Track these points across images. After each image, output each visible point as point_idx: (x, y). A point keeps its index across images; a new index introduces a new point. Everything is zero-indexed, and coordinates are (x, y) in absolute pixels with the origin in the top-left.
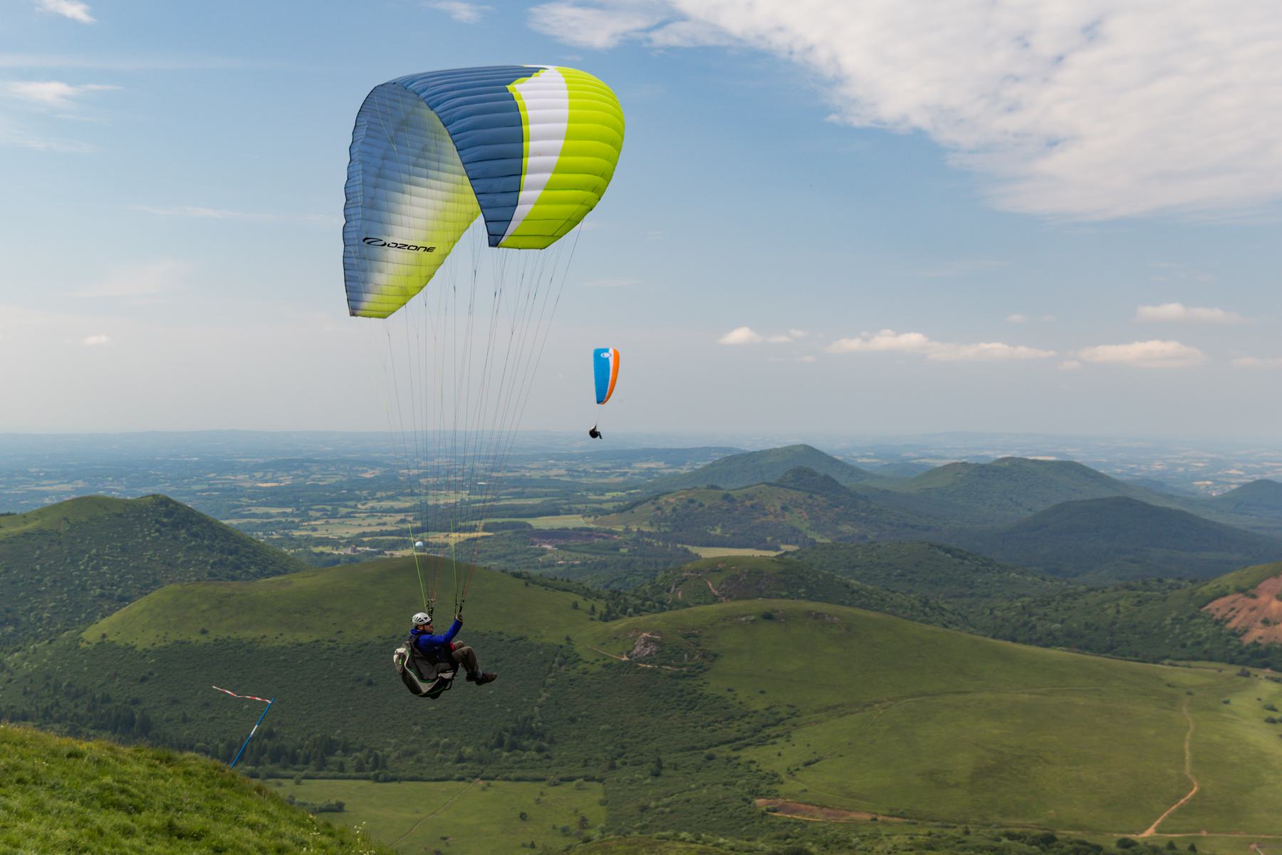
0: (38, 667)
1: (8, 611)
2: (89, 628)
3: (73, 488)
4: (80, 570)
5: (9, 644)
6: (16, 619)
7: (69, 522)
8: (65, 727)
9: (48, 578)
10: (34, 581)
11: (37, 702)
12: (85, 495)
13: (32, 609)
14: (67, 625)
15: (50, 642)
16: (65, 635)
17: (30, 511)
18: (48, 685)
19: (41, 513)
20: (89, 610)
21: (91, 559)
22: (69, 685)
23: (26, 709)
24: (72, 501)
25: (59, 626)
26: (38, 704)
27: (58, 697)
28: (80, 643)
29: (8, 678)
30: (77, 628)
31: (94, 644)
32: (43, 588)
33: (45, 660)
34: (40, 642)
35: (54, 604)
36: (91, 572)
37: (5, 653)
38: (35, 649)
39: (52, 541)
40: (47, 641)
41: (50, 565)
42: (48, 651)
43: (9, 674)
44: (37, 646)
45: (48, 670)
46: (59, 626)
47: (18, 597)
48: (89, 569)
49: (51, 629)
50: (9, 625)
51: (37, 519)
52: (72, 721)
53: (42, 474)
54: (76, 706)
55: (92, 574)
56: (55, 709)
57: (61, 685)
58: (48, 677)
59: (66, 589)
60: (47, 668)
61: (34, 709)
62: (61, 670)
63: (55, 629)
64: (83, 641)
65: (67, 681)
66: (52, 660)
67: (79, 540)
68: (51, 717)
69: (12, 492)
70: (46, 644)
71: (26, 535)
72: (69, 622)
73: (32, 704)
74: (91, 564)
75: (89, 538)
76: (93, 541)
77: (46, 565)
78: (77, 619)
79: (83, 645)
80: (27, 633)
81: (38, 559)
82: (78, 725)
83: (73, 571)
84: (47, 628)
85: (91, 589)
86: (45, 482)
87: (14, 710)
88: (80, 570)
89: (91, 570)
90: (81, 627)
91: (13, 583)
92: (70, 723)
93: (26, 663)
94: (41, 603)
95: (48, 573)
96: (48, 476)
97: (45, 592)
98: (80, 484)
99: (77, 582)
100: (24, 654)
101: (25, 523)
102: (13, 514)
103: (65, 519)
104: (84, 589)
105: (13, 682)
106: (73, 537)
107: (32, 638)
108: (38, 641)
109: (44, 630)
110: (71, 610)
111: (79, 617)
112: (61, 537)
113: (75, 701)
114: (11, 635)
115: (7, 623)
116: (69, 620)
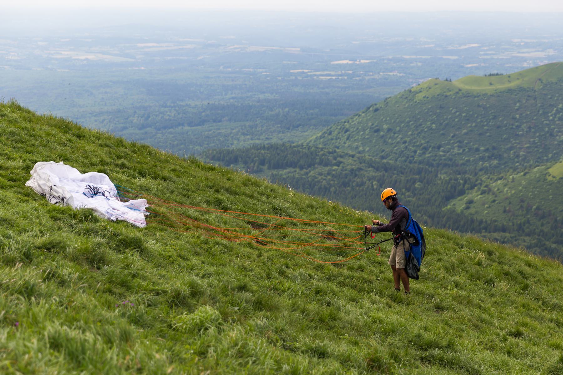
0: (515, 193)
1: (494, 148)
2: (555, 165)
3: (545, 55)
4: (549, 120)
5: (494, 174)
6: (500, 155)
7: (542, 82)
8: (534, 240)
9: (525, 125)
10: (514, 127)
11: (513, 219)
12: (554, 62)
13: (511, 148)
14: (538, 162)
15: (525, 175)
16: (536, 170)
17: (513, 72)
18: (522, 207)
19: (521, 75)
20: (555, 152)
21: (558, 112)
22: (538, 208)
23: (505, 223)
24: (546, 65)
25: (532, 162)
26: (515, 221)
27: (529, 216)
28: (547, 176)
29: (492, 199)
30: (545, 165)
31: (558, 178)
32: (521, 133)
33: (520, 188)
34: (517, 174)
35: (528, 145)
36: (557, 122)
37: (491, 180)
38: (513, 178)
39: (529, 96)
40: (522, 174)
41: (527, 115)
42: (523, 181)
43: (494, 196)
44: (515, 176)
45: (522, 195)
46: (532, 162)
47: (502, 138)
48: (556, 119)
49: (525, 164)
50: (495, 159)
51: (518, 79)
52: (539, 236)
53: (522, 44)
54: (542, 225)
55: (559, 124)
56: (527, 225)
57: (532, 208)
58: (522, 201)
59: (538, 134)
60: (521, 194)
61: (511, 224)
62: (532, 196)
63: (528, 164)
64: (549, 176)
65: (537, 204)
66: (526, 188)
67: (549, 96)
68: (523, 231)
69: (500, 57)
70: (522, 176)
71: (510, 91)
72: (539, 160)
73: (509, 220)
74: (558, 116)
75: (557, 95)
76: (560, 98)
77: (524, 115)
78: (545, 158)
79: (550, 178)
80: (508, 166)
81: (518, 110)
82: (543, 239)
83: (544, 121)
84: (522, 163)
85: (557, 135)
86: (525, 50)
87: (496, 223)
88: (549, 120)
89: (558, 121)
90: (549, 164)
91: (498, 127)
92: (537, 237)
93: (506, 189)
94: (519, 143)
95: (525, 121)
96: (527, 45)
97: (522, 135)
98: (551, 52)
99: (547, 129)
100: (505, 181)
101: (510, 82)
102: (501, 74)
103: (540, 80)
104: (551, 135)
105: (497, 202)
106: (545, 94)
107: (511, 170)
108: (516, 173)
109: (520, 165)
110: (541, 150)
111: (547, 156)
112: (536, 93)
113: (542, 220)
114: (496, 167)
115: (493, 158)
116: (539, 158)
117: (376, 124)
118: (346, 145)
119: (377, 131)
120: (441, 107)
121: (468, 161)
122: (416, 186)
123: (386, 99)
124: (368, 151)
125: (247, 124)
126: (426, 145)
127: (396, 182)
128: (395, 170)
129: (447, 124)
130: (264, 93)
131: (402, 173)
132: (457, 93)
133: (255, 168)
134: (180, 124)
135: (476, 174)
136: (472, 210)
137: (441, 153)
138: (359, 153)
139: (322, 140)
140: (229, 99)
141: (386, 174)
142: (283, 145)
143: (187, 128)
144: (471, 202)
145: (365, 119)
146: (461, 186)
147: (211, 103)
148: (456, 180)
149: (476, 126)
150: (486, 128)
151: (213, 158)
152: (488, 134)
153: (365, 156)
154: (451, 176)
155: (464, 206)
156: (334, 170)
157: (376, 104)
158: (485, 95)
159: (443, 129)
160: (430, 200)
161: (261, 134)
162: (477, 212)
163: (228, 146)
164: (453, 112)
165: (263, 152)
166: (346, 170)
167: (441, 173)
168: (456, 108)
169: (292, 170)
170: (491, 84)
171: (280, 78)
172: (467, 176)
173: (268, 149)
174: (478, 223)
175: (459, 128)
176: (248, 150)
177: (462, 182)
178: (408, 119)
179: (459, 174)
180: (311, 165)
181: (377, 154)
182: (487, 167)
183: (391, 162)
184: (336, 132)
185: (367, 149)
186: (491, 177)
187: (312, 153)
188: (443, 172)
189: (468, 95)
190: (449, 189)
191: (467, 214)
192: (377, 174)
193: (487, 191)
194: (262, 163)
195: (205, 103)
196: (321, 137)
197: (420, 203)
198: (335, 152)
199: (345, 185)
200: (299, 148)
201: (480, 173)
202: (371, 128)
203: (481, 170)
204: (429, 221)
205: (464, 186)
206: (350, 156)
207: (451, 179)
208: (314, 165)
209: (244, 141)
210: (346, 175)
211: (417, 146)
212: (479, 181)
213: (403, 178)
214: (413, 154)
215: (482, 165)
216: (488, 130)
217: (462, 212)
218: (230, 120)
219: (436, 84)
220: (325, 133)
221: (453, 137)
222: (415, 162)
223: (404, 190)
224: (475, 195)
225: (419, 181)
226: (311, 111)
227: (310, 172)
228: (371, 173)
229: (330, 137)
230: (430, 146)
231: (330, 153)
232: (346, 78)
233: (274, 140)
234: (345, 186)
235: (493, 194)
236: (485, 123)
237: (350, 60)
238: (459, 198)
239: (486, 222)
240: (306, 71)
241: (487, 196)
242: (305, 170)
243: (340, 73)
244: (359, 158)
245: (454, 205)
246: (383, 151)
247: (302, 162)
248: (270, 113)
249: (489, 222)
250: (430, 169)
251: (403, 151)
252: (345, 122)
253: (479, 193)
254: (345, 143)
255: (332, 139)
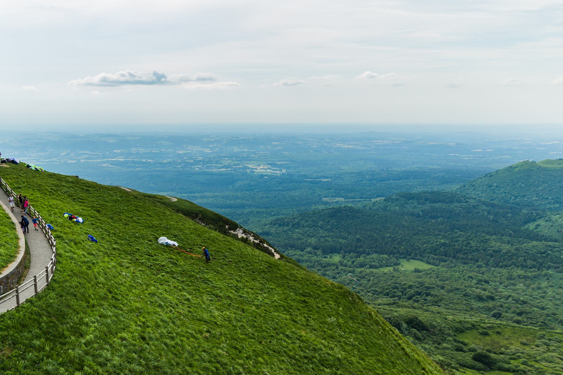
1: (557, 198)
6: (561, 202)
23: (557, 238)
37: (553, 214)
73: (560, 236)
100: (560, 216)
114: (557, 208)
117: (490, 183)
118: (473, 193)
119: (490, 186)
120: (528, 176)
121: (541, 204)
122: (508, 215)
123: (498, 170)
124: (484, 196)
125: (422, 180)
126: (517, 194)
127: (497, 212)
128: (497, 207)
129: (530, 185)
130: (433, 165)
131: (502, 209)
132: (538, 168)
133: (422, 202)
134: (388, 179)
135: (544, 211)
136: (539, 230)
137: (526, 199)
138: (479, 197)
139: (460, 190)
140: (415, 168)
141: (492, 208)
142: (438, 191)
143: (392, 181)
144: (538, 225)
145: (484, 180)
146: (534, 217)
147: (405, 169)
148: (532, 213)
149: (547, 186)
150: (553, 187)
151: (402, 197)
152: (555, 190)
153: (481, 199)
154: (530, 212)
155: (534, 227)
156: (464, 205)
157: (491, 173)
158: (556, 169)
159: (528, 187)
160: (515, 223)
161: (429, 186)
162: (541, 231)
163: (411, 191)
164: (535, 178)
165: (427, 194)
166: (470, 205)
167: (524, 210)
168: (537, 176)
169: (442, 204)
170: (559, 164)
171: (443, 158)
172: (539, 211)
173: (430, 193)
174: (541, 237)
175: (538, 187)
176: (419, 194)
177: (535, 214)
178: (508, 181)
179: (534, 210)
180: (452, 202)
181: (489, 198)
182: (552, 208)
183: (496, 202)
184: (468, 186)
185: (484, 195)
186: (553, 213)
187: (453, 196)
188: (525, 209)
189: (545, 169)
190: (527, 218)
191: (535, 231)
192: (487, 208)
193: (549, 220)
194: (426, 200)
195: (403, 169)
196: (459, 189)
197: (509, 224)
198: (465, 196)
199: (469, 213)
200: (446, 194)
201: (547, 210)
202: (487, 185)
203: (548, 209)
204: (513, 234)
205: (536, 217)
206: (473, 198)
207: (529, 213)
208: (453, 202)
209: (420, 189)
210: (470, 208)
211: (513, 195)
212: (545, 215)
213: (501, 211)
214: (509, 199)
215: (549, 206)
216: (555, 188)
217: (532, 230)
218: (414, 178)
219: (526, 164)
220: (462, 186)
221: (533, 191)
222: (510, 203)
223: (501, 217)
224: (541, 222)
225: (510, 213)
226: (457, 175)
227: (451, 205)
228: (484, 207)
229: (464, 188)
230: (520, 195)
231: (462, 196)
232: (478, 158)
233: (435, 189)
234: (469, 214)
235: (552, 222)
236: (554, 185)
237: (482, 150)
238: (532, 223)
239: (546, 236)
240: (457, 155)
241: (548, 223)
242: (448, 204)
243: (475, 156)
244: (478, 200)
245: (529, 226)
246: (492, 197)
247: (447, 200)
248: (435, 175)
249: (547, 236)
250: (518, 207)
251: (504, 197)
252: (473, 181)
253: (544, 221)
254: (472, 192)
255: (465, 190)
